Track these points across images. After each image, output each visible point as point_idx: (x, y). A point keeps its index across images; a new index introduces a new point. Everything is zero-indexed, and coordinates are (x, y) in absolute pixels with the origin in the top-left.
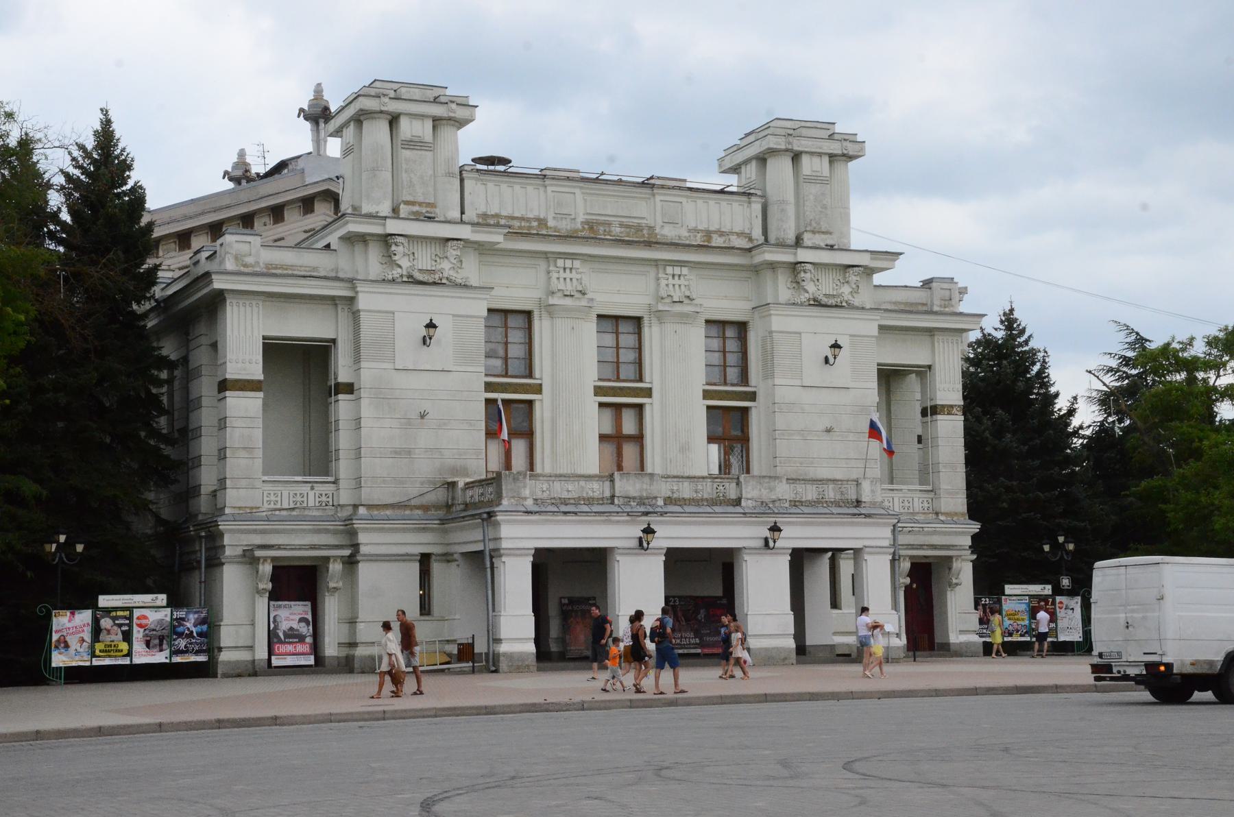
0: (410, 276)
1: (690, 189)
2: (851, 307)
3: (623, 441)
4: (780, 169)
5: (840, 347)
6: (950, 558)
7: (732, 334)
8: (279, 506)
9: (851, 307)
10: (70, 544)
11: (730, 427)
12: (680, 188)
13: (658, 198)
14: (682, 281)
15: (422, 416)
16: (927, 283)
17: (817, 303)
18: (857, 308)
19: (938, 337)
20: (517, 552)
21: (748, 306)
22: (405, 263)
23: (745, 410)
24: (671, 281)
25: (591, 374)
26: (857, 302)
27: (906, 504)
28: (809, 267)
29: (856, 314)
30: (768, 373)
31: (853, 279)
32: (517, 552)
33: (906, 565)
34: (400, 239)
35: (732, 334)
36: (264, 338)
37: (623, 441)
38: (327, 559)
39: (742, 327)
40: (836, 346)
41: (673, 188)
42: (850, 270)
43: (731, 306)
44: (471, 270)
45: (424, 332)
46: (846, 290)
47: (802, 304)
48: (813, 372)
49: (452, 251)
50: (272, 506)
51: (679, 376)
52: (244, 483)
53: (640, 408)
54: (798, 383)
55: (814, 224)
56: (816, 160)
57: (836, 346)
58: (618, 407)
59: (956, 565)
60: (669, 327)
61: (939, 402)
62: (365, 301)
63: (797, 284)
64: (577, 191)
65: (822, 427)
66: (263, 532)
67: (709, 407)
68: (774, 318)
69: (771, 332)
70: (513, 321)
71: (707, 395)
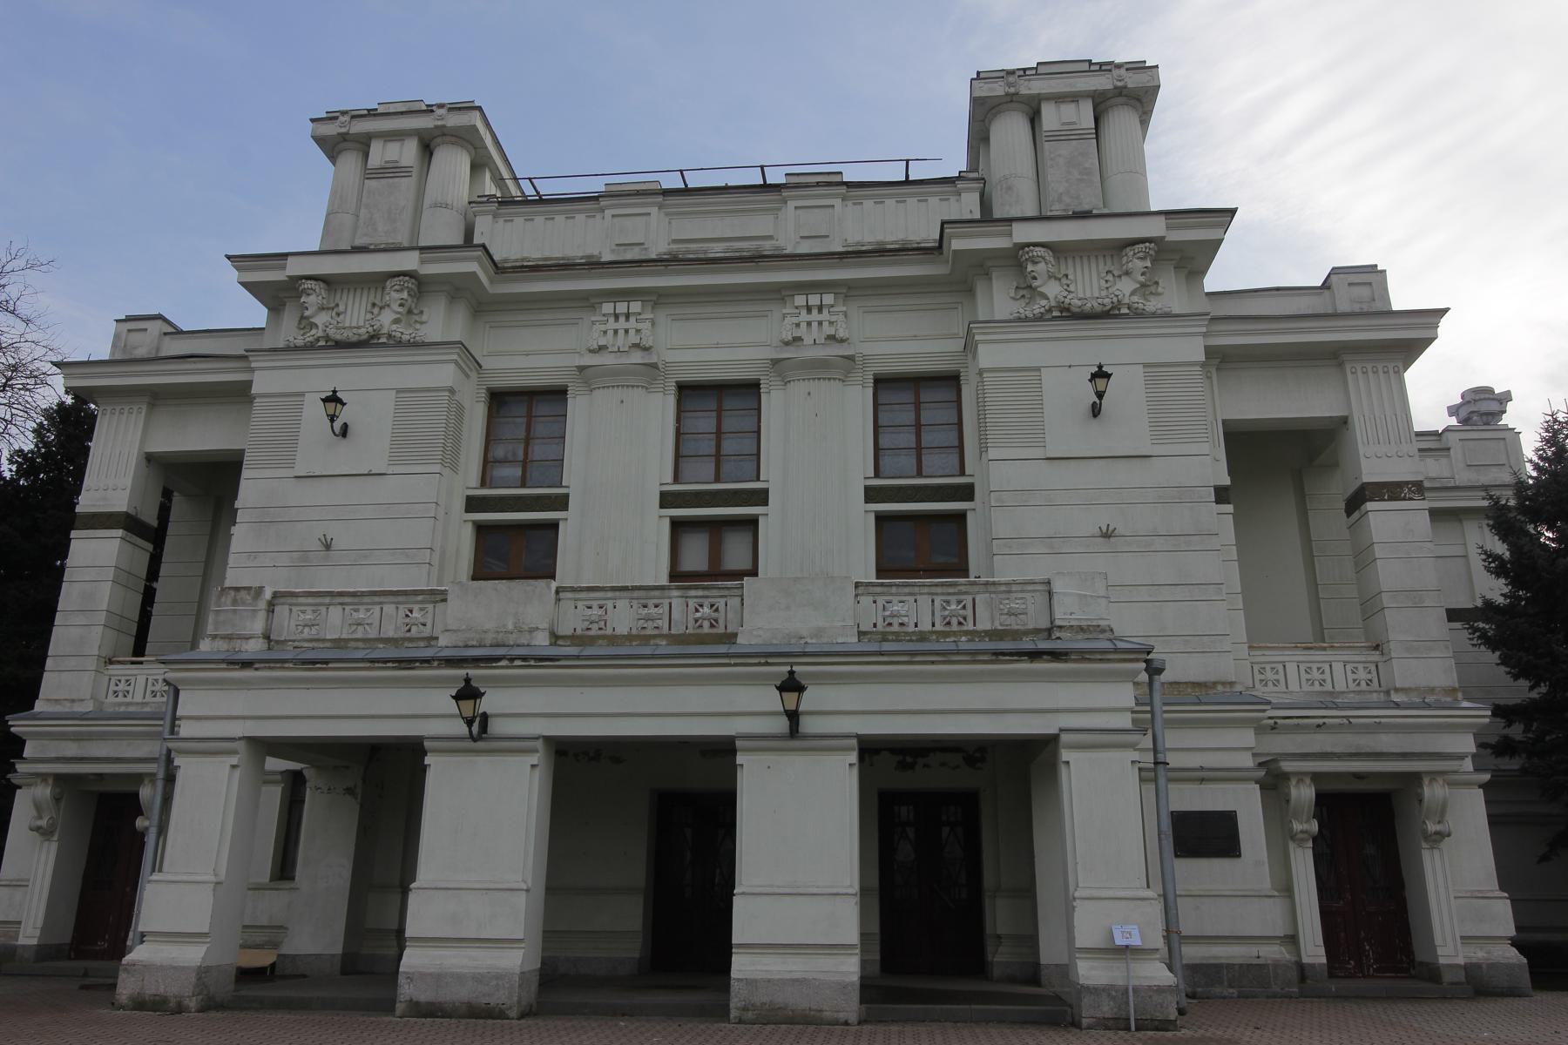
0: (327, 338)
1: (849, 185)
2: (1138, 314)
4: (1010, 132)
5: (1108, 376)
6: (1415, 778)
8: (129, 699)
9: (1138, 314)
12: (829, 184)
13: (791, 204)
14: (825, 315)
15: (328, 547)
16: (1326, 285)
17: (1068, 314)
18: (1154, 315)
20: (209, 748)
21: (958, 345)
22: (321, 319)
23: (961, 517)
24: (804, 316)
26: (1152, 305)
27: (1316, 675)
28: (1039, 251)
30: (983, 448)
31: (1138, 265)
32: (209, 748)
33: (1304, 794)
34: (308, 284)
36: (150, 458)
38: (139, 778)
39: (951, 380)
40: (1101, 374)
41: (818, 184)
42: (1129, 251)
44: (439, 322)
45: (345, 415)
46: (1125, 287)
47: (1040, 318)
48: (1066, 430)
49: (395, 295)
50: (120, 699)
51: (819, 470)
52: (72, 663)
53: (752, 523)
54: (1039, 453)
55: (1066, 199)
56: (1068, 111)
57: (1101, 374)
58: (716, 527)
59: (1433, 792)
60: (798, 388)
61: (1366, 479)
62: (263, 382)
63: (1028, 290)
64: (654, 210)
65: (1096, 531)
66: (78, 738)
67: (881, 518)
68: (981, 348)
69: (981, 372)
71: (872, 494)
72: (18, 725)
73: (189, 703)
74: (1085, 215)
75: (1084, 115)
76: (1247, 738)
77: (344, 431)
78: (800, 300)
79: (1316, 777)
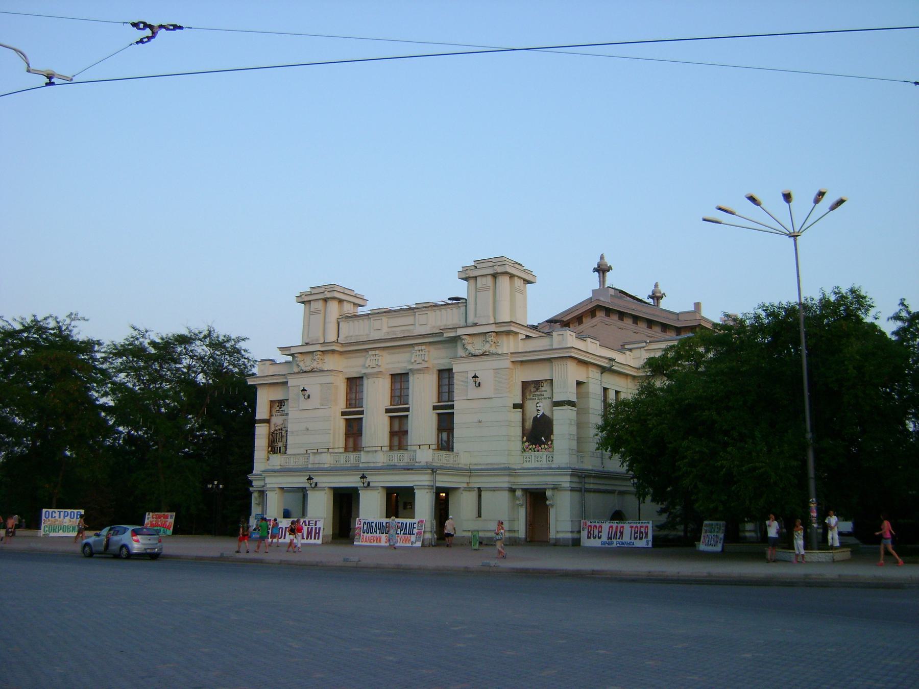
2: (493, 354)
3: (399, 435)
7: (445, 375)
10: (218, 485)
11: (446, 423)
19: (555, 363)
20: (273, 489)
25: (386, 403)
29: (495, 358)
32: (273, 489)
33: (519, 493)
35: (445, 375)
37: (399, 435)
43: (443, 363)
56: (484, 279)
67: (439, 414)
70: (354, 383)
72: (250, 477)
73: (268, 480)
74: (476, 325)
75: (489, 280)
76: (507, 479)
77: (309, 397)
78: (416, 348)
79: (523, 489)
